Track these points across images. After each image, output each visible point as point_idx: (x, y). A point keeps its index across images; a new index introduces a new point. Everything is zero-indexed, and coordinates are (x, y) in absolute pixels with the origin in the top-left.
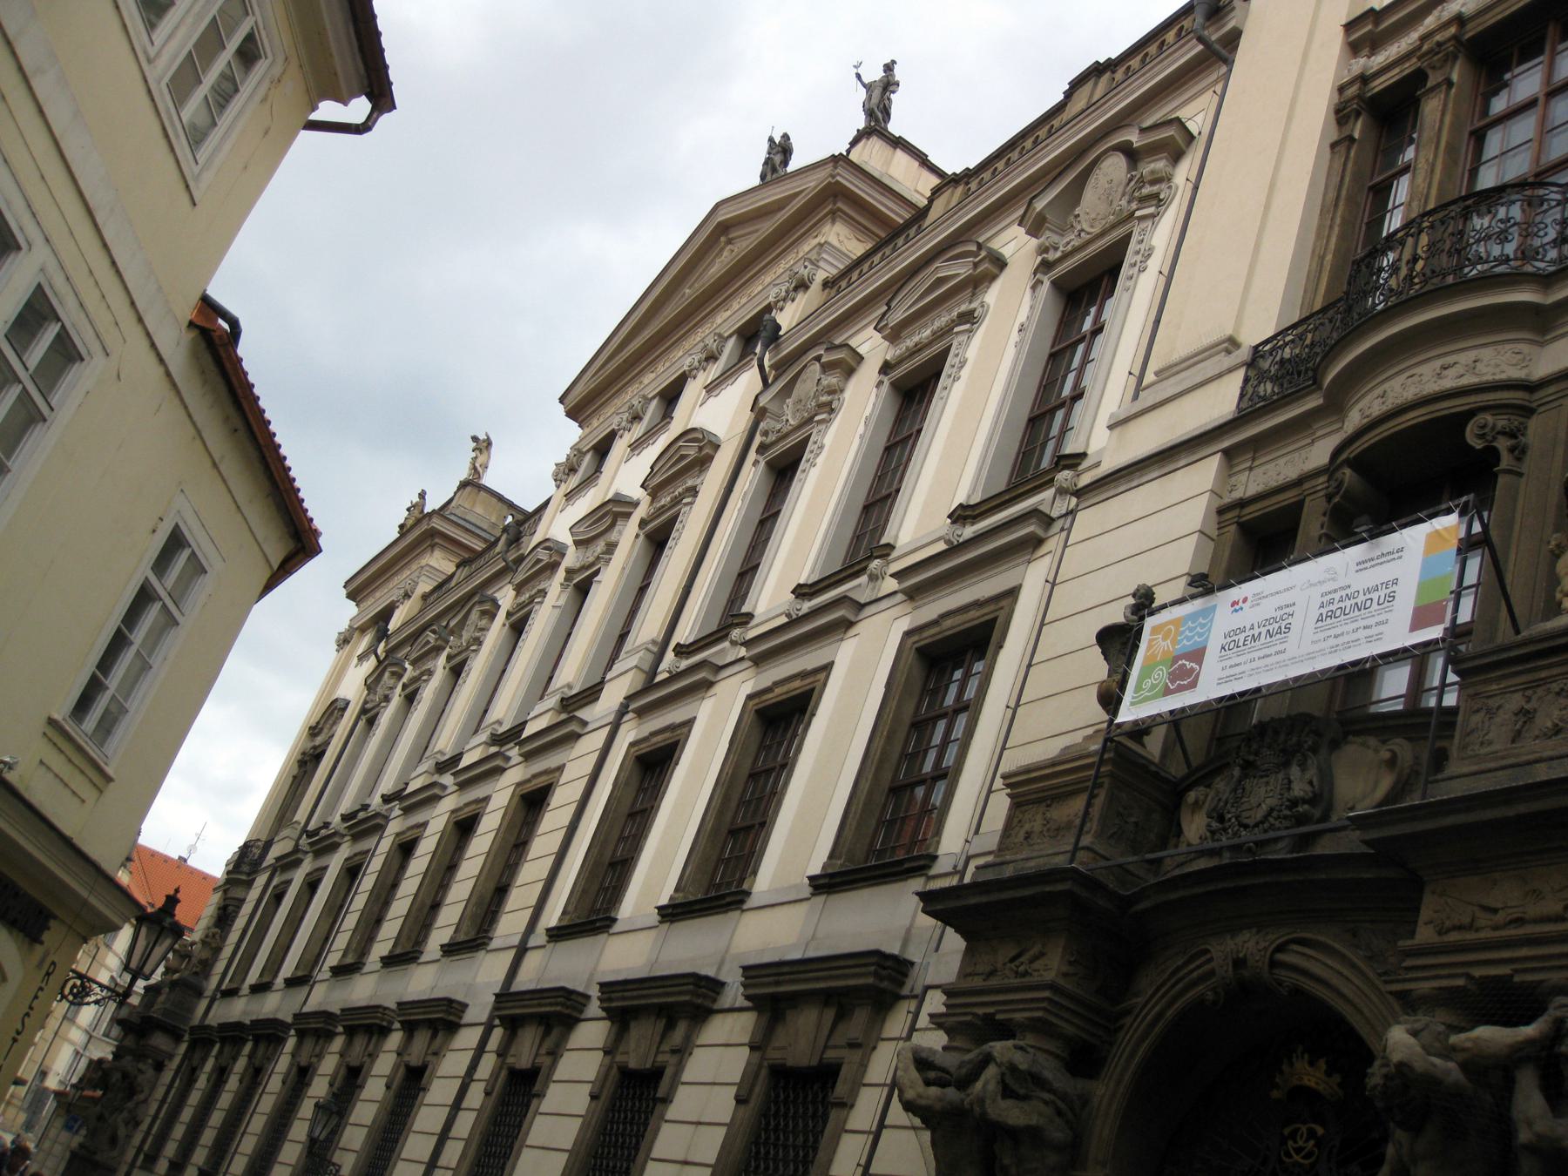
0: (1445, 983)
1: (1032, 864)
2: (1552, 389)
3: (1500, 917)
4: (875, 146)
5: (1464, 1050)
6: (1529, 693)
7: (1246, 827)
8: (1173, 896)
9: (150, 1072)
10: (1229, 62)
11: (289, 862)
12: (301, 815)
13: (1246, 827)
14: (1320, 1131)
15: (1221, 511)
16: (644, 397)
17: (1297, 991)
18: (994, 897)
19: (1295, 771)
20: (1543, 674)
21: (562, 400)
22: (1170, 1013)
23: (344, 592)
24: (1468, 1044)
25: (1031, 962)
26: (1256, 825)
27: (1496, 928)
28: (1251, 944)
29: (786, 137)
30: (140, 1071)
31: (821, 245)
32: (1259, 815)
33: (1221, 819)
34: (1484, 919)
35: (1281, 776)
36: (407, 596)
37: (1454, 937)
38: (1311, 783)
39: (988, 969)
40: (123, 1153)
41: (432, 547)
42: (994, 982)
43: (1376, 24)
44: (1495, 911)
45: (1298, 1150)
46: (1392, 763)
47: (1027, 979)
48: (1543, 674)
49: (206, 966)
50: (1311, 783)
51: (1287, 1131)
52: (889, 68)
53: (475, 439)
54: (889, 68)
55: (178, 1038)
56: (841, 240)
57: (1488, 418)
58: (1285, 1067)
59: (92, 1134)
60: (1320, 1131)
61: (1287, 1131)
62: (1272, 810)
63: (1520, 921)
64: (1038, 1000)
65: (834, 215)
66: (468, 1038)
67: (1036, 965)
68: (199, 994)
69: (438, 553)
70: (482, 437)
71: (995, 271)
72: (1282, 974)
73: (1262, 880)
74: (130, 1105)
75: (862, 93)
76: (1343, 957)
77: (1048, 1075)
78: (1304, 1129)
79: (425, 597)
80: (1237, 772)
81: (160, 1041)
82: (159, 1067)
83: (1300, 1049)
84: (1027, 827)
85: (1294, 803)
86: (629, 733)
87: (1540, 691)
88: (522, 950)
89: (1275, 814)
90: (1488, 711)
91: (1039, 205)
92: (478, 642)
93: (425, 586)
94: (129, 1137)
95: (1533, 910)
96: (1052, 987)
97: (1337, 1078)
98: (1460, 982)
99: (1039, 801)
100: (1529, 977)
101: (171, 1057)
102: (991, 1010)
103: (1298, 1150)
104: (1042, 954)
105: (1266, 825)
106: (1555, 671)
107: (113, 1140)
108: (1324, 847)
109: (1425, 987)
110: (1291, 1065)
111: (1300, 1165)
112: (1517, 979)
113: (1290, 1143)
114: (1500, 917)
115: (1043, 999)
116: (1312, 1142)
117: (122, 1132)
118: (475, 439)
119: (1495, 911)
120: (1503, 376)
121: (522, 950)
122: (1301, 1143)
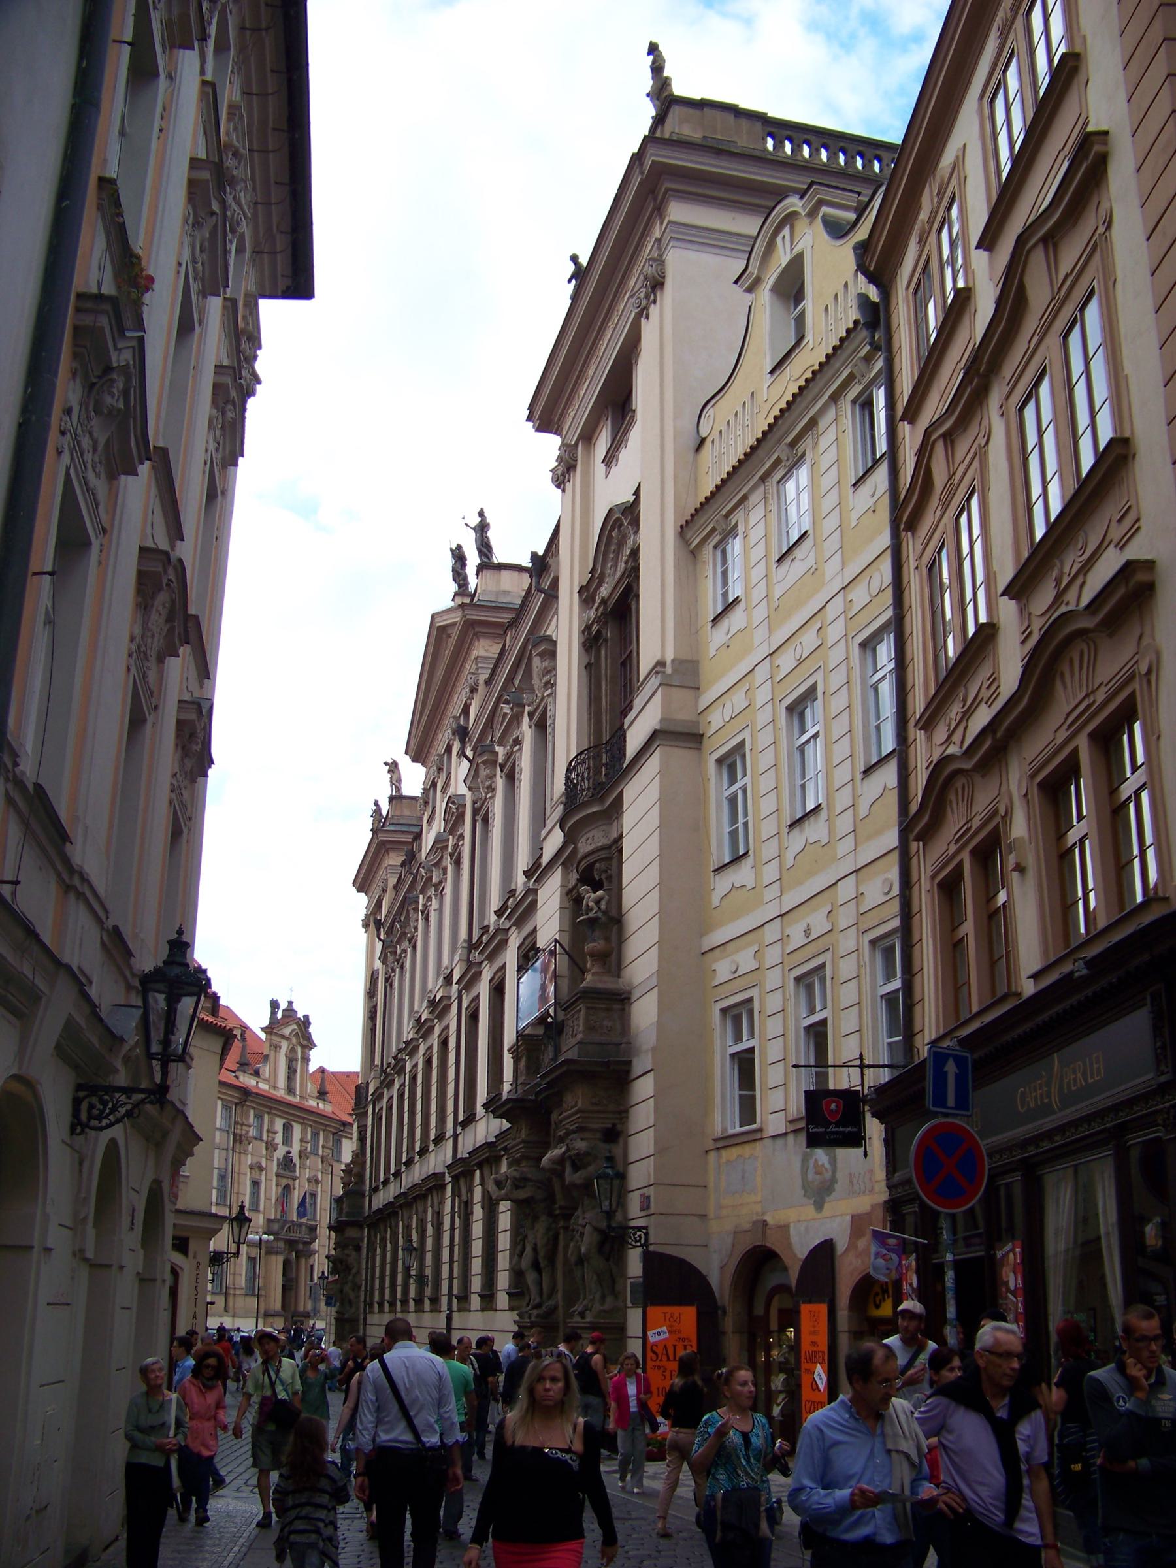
4: (487, 574)
9: (354, 1253)
10: (556, 597)
11: (378, 1096)
12: (377, 1061)
15: (567, 894)
16: (439, 755)
21: (406, 753)
23: (354, 889)
29: (459, 547)
30: (348, 1255)
31: (476, 659)
36: (384, 891)
40: (358, 1308)
41: (387, 851)
43: (588, 591)
49: (361, 1177)
52: (481, 514)
53: (386, 764)
54: (481, 514)
55: (361, 1227)
56: (485, 649)
59: (342, 1304)
65: (477, 636)
66: (449, 1188)
68: (363, 1195)
69: (392, 854)
70: (390, 761)
71: (520, 709)
74: (350, 1277)
75: (473, 533)
77: (529, 1176)
79: (395, 887)
81: (351, 1233)
82: (358, 1249)
86: (465, 1004)
88: (455, 1137)
91: (517, 683)
92: (416, 929)
93: (393, 881)
94: (358, 1297)
96: (523, 1142)
101: (362, 1240)
107: (350, 1302)
117: (352, 1295)
118: (386, 764)
121: (455, 1137)
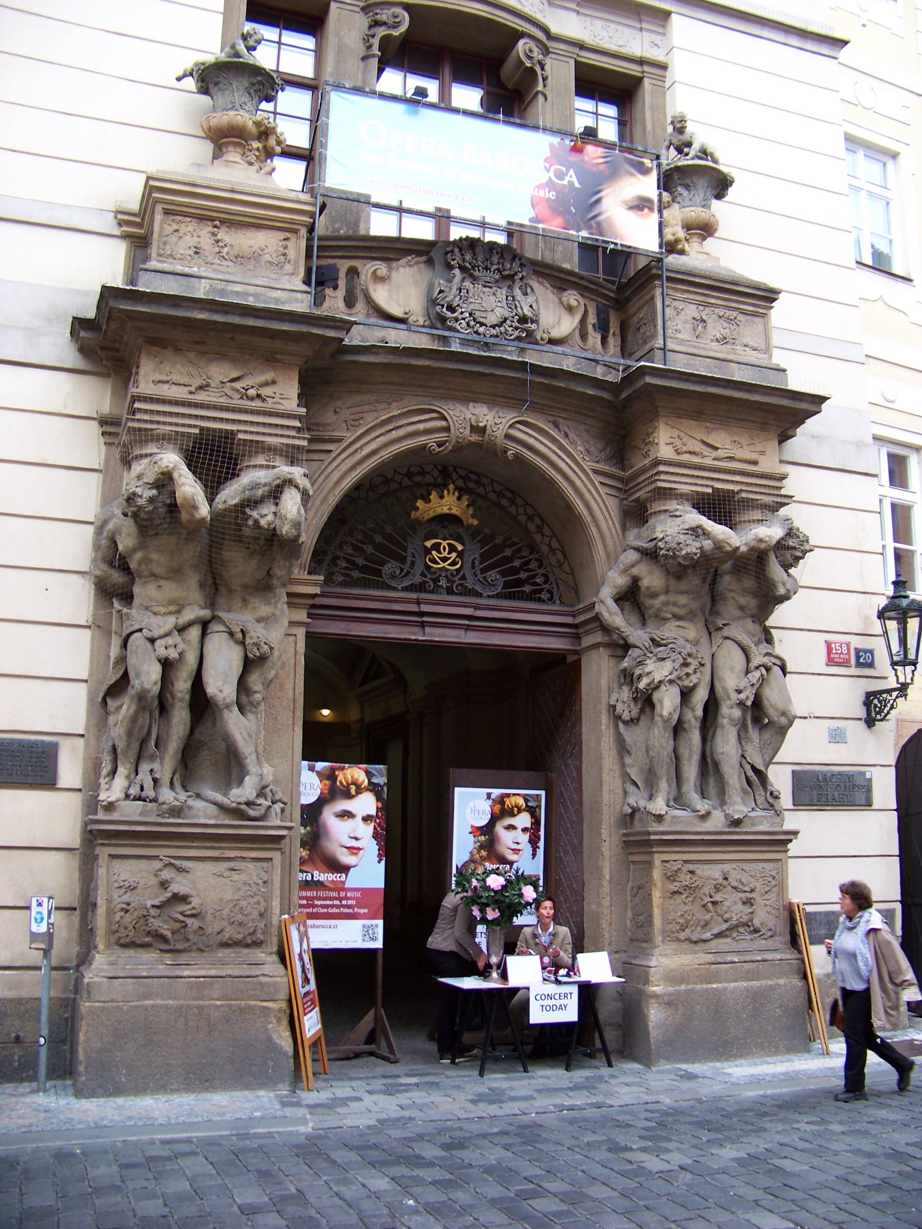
0: (699, 489)
1: (238, 288)
2: (562, 46)
3: (720, 453)
5: (766, 542)
6: (701, 308)
7: (482, 324)
8: (414, 362)
13: (482, 324)
14: (460, 547)
17: (517, 456)
18: (237, 320)
19: (517, 292)
20: (712, 301)
22: (385, 454)
24: (767, 539)
25: (262, 385)
26: (493, 327)
27: (714, 459)
28: (496, 420)
32: (492, 319)
33: (452, 309)
34: (706, 451)
35: (504, 291)
37: (686, 458)
38: (531, 306)
39: (197, 382)
42: (201, 397)
44: (717, 449)
45: (444, 560)
46: (570, 309)
47: (257, 404)
48: (712, 301)
50: (531, 306)
51: (429, 544)
57: (532, 44)
58: (434, 496)
60: (460, 548)
61: (429, 544)
62: (505, 320)
63: (731, 458)
64: (288, 427)
67: (266, 391)
72: (510, 443)
73: (514, 375)
76: (554, 440)
78: (445, 543)
80: (457, 272)
83: (451, 487)
84: (189, 241)
85: (523, 320)
87: (708, 310)
89: (508, 322)
90: (675, 309)
95: (740, 454)
97: (471, 511)
98: (710, 491)
99: (201, 219)
100: (751, 496)
102: (234, 427)
103: (444, 560)
104: (274, 382)
105: (502, 329)
106: (720, 302)
108: (532, 358)
109: (685, 489)
110: (442, 497)
111: (448, 570)
112: (744, 495)
113: (434, 553)
114: (720, 453)
115: (294, 428)
116: (454, 555)
119: (717, 449)
120: (534, 15)
122: (445, 554)
